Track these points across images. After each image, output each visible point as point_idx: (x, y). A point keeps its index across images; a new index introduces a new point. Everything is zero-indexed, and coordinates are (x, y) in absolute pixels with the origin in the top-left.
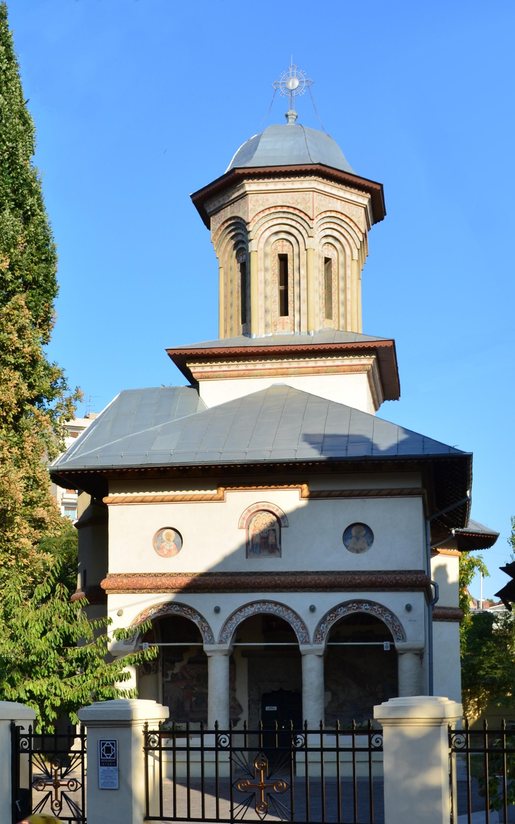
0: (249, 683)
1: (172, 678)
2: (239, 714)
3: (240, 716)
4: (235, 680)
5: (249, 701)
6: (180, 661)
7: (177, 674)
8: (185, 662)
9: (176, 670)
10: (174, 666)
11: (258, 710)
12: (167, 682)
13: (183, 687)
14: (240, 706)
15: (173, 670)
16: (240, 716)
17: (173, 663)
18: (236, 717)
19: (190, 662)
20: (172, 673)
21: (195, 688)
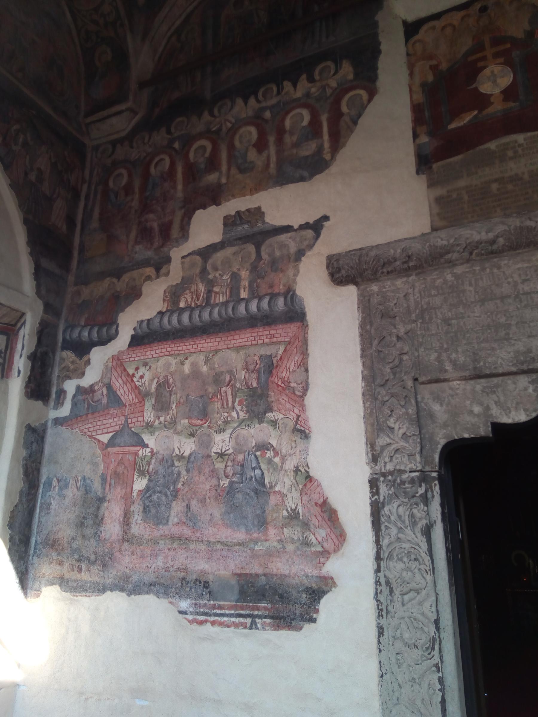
0: (371, 394)
1: (74, 404)
2: (326, 554)
3: (333, 567)
4: (305, 390)
5: (373, 484)
6: (103, 342)
7: (91, 390)
8: (122, 341)
9: (91, 376)
10: (88, 362)
11: (427, 532)
12: (58, 421)
13: (105, 438)
14: (329, 514)
15: (83, 374)
16: (333, 567)
17: (82, 349)
18: (313, 572)
19: (137, 341)
20: (79, 389)
21: (147, 438)
